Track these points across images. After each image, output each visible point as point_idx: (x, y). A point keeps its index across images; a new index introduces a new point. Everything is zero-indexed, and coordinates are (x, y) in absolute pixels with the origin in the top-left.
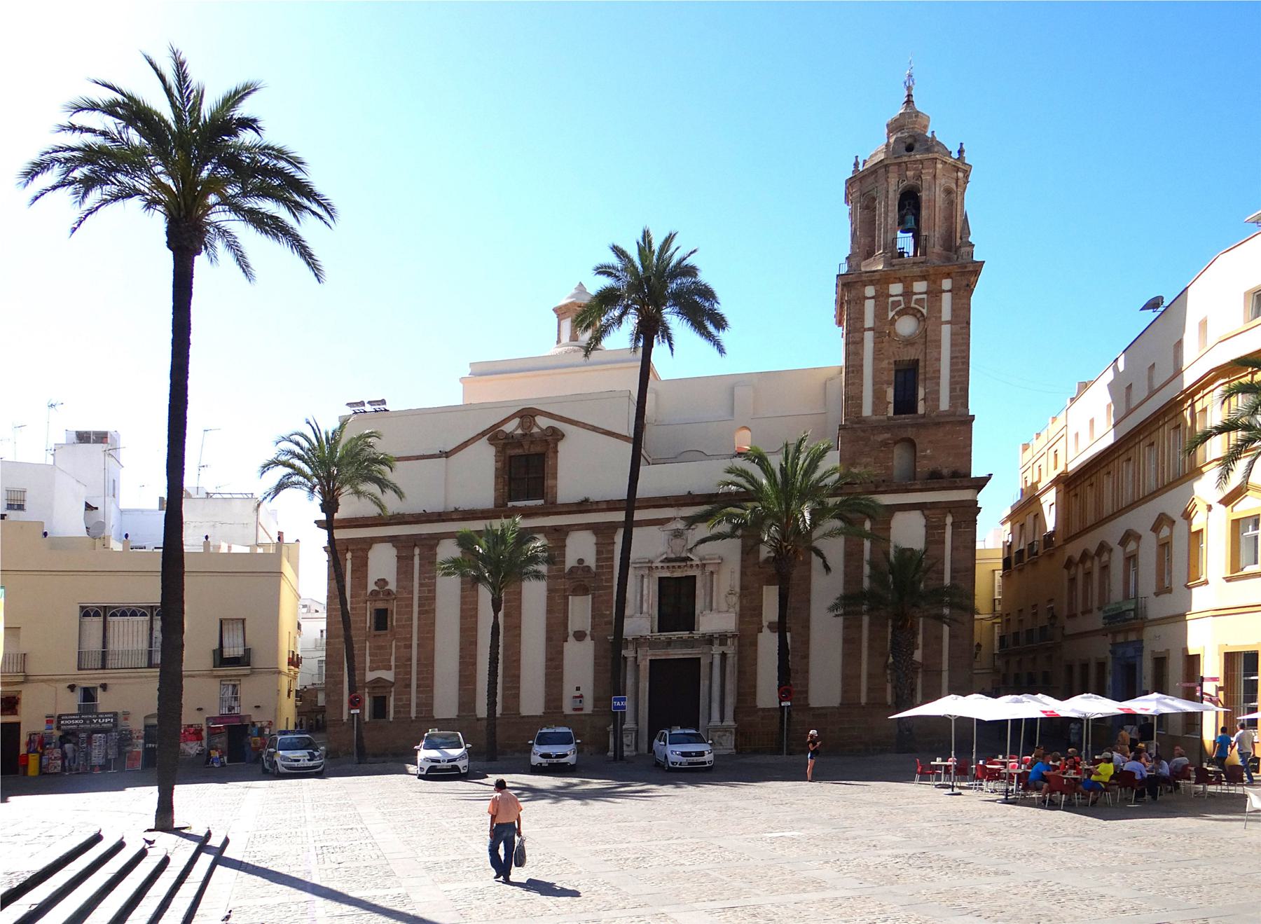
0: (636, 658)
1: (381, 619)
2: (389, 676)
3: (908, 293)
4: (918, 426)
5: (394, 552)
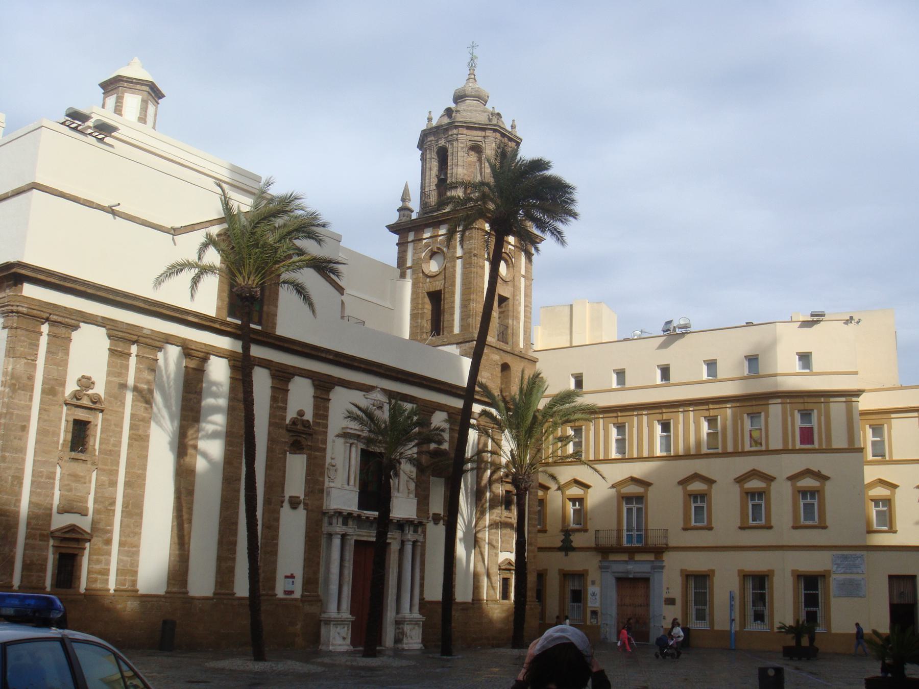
2: (85, 523)
5: (106, 343)
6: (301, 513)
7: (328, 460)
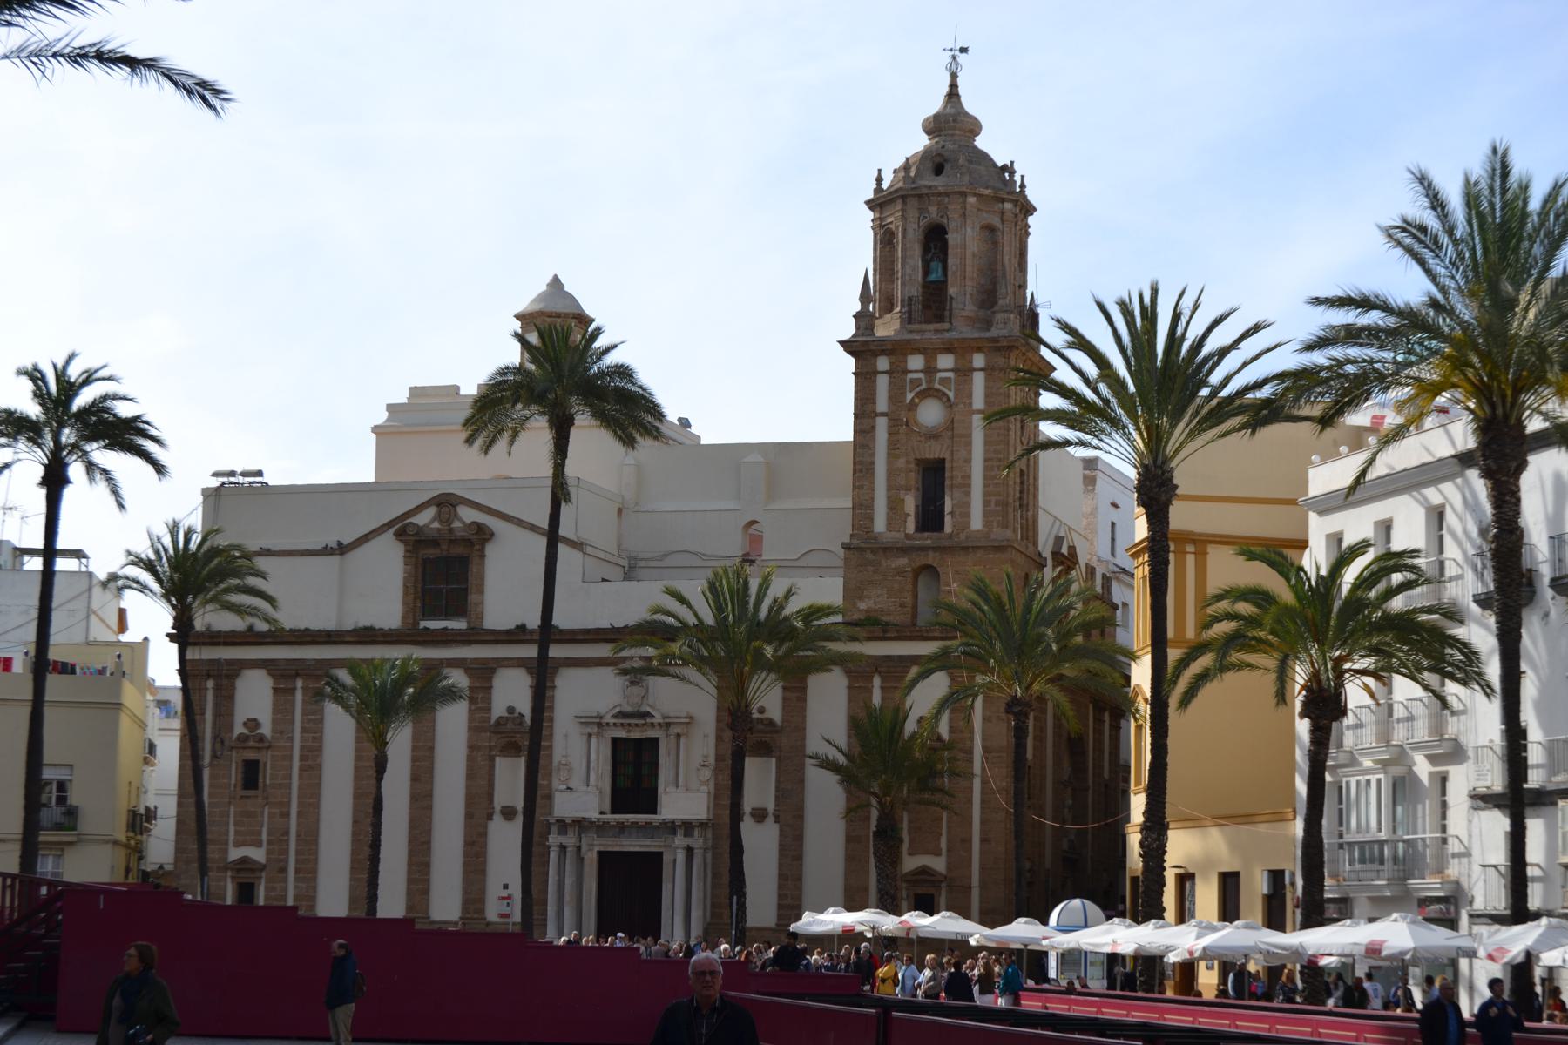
0: (579, 848)
1: (251, 775)
2: (258, 855)
3: (930, 370)
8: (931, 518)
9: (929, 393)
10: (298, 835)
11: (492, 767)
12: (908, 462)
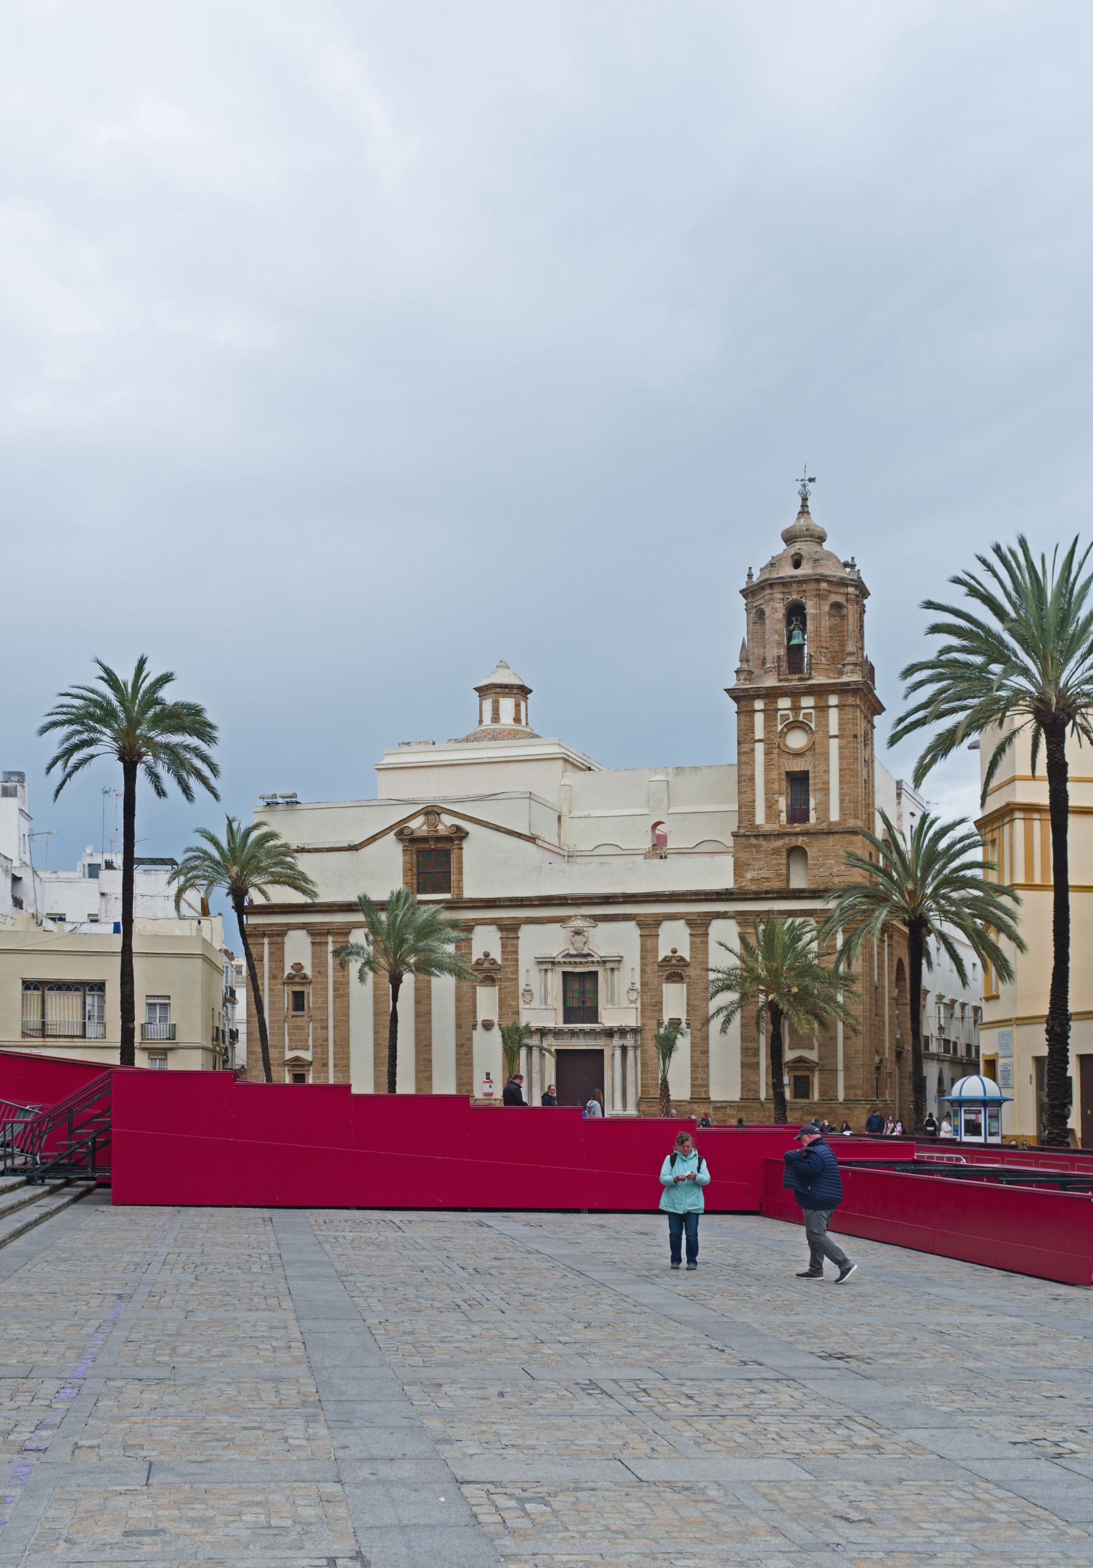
1: (299, 1001)
2: (307, 1055)
3: (796, 708)
4: (806, 833)
6: (496, 1034)
7: (522, 987)
8: (798, 814)
9: (796, 725)
10: (335, 1042)
11: (475, 993)
12: (780, 774)
